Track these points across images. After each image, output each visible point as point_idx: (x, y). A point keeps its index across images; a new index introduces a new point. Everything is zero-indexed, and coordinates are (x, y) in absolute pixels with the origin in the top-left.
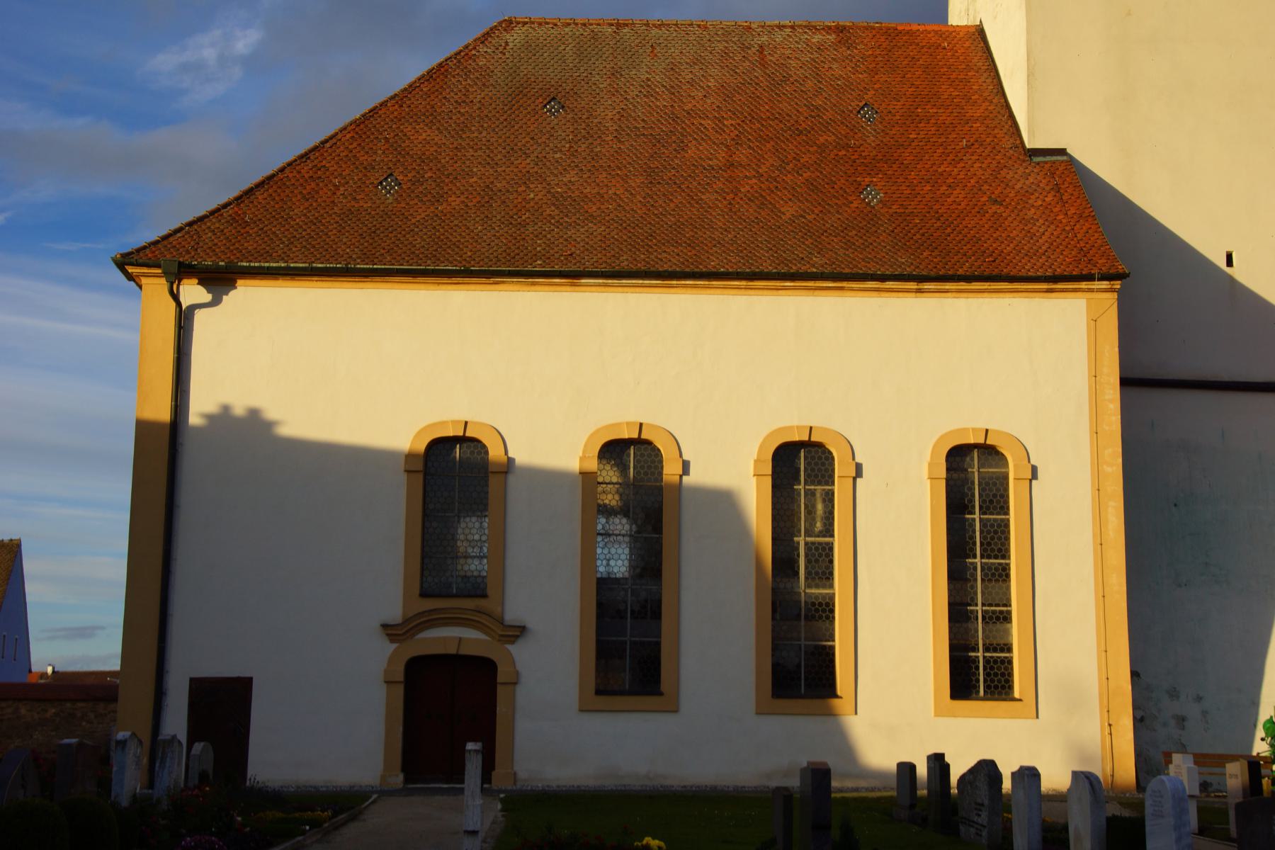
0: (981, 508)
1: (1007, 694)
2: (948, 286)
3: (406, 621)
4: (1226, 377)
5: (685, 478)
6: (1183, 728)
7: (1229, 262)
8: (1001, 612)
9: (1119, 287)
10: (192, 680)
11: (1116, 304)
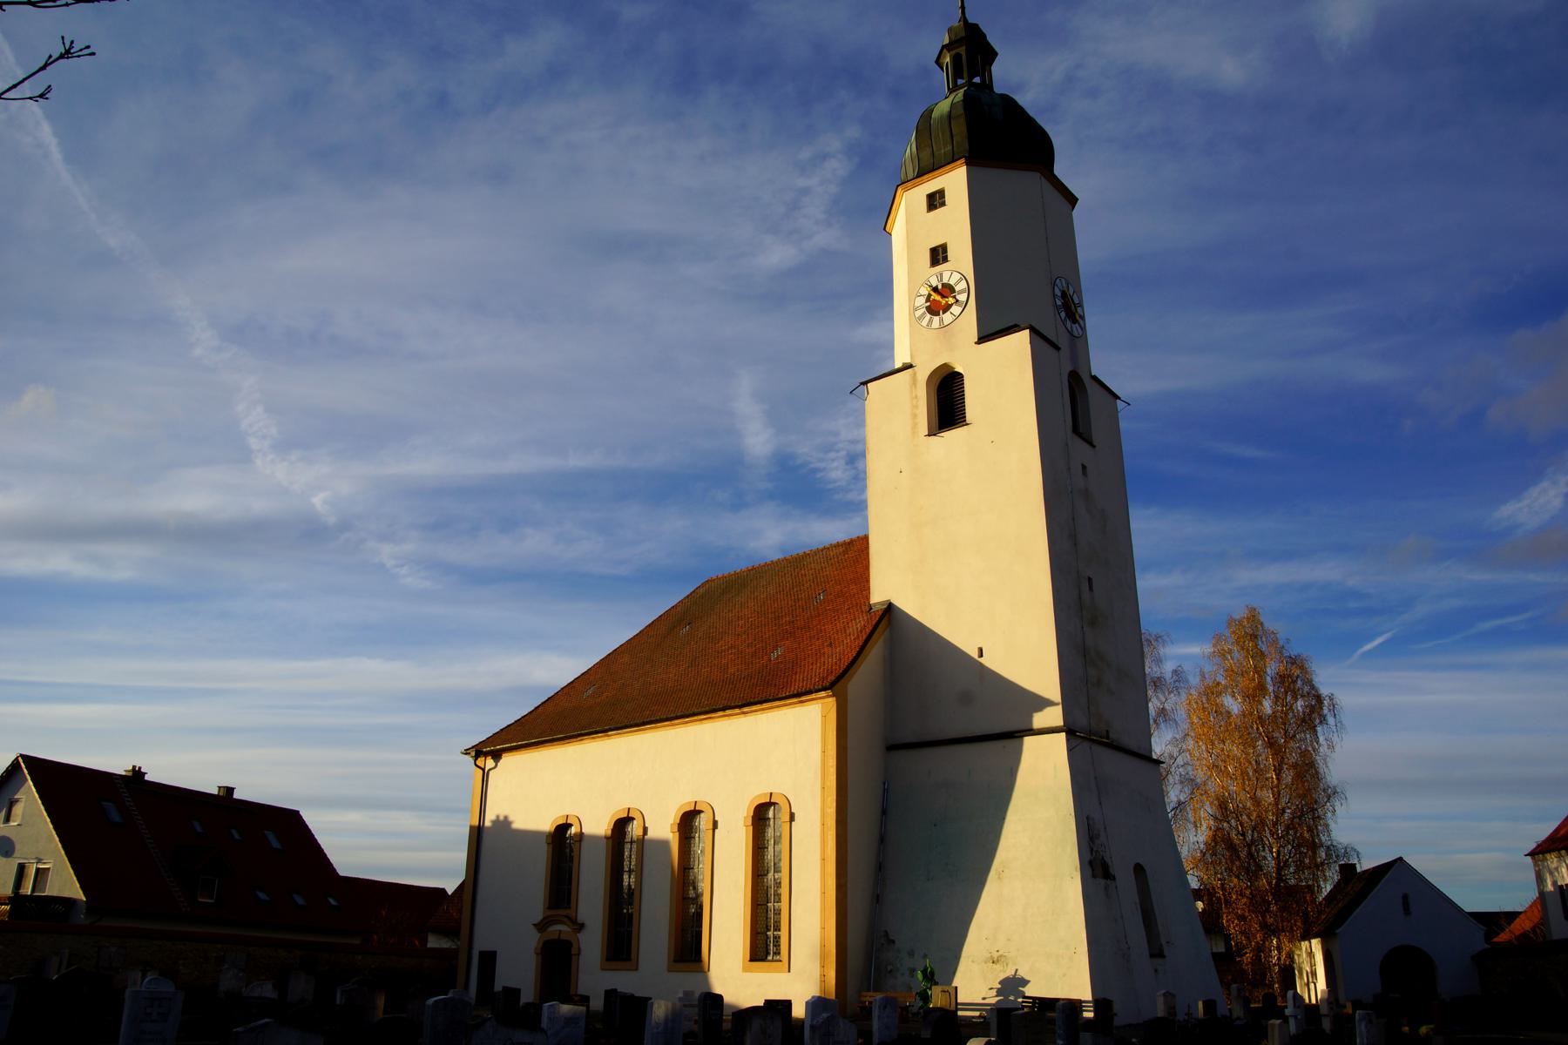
2: (754, 708)
3: (544, 918)
4: (978, 732)
5: (646, 837)
6: (913, 976)
7: (981, 655)
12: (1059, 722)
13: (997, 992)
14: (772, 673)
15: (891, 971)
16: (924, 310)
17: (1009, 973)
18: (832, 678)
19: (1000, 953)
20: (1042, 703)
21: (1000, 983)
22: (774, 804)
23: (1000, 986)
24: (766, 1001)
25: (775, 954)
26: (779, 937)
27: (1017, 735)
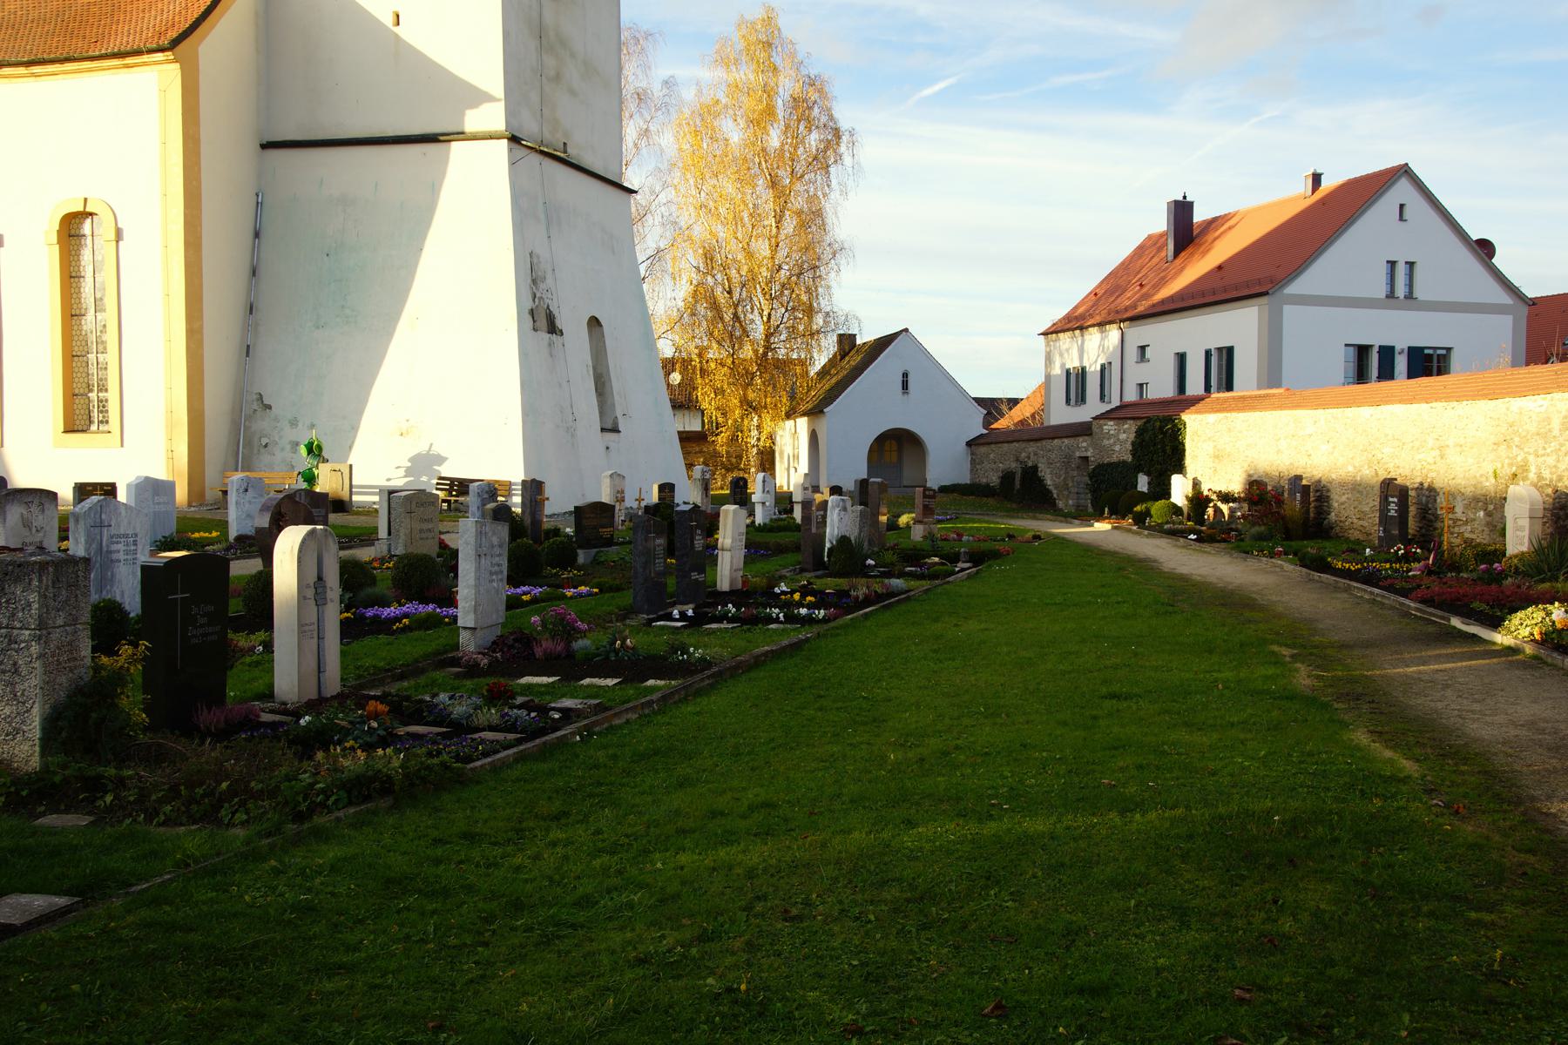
4: (390, 133)
9: (173, 57)
11: (180, 74)
12: (498, 123)
13: (405, 471)
14: (78, 18)
15: (266, 446)
17: (422, 448)
18: (173, 34)
20: (478, 97)
21: (409, 461)
22: (91, 214)
23: (409, 464)
24: (76, 484)
25: (100, 422)
26: (107, 401)
27: (441, 138)
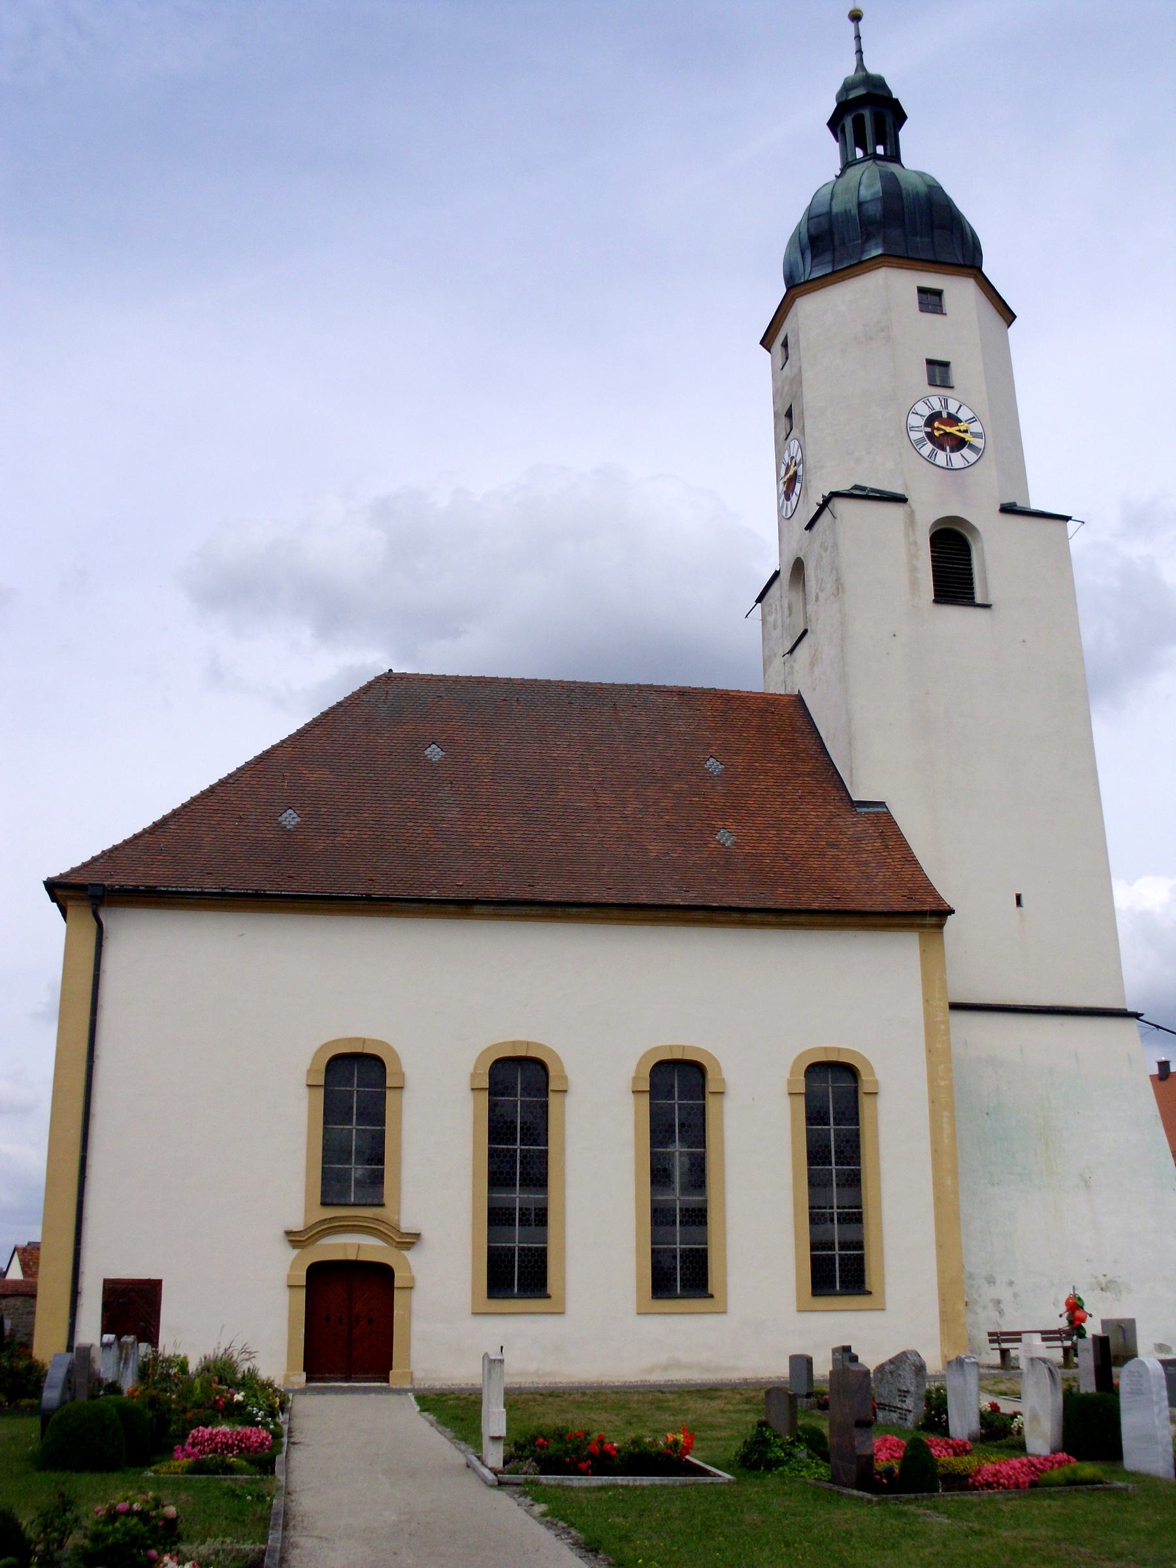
0: (835, 1119)
1: (859, 1288)
3: (308, 1229)
8: (854, 1213)
10: (106, 1281)
16: (923, 434)
19: (1108, 1278)
